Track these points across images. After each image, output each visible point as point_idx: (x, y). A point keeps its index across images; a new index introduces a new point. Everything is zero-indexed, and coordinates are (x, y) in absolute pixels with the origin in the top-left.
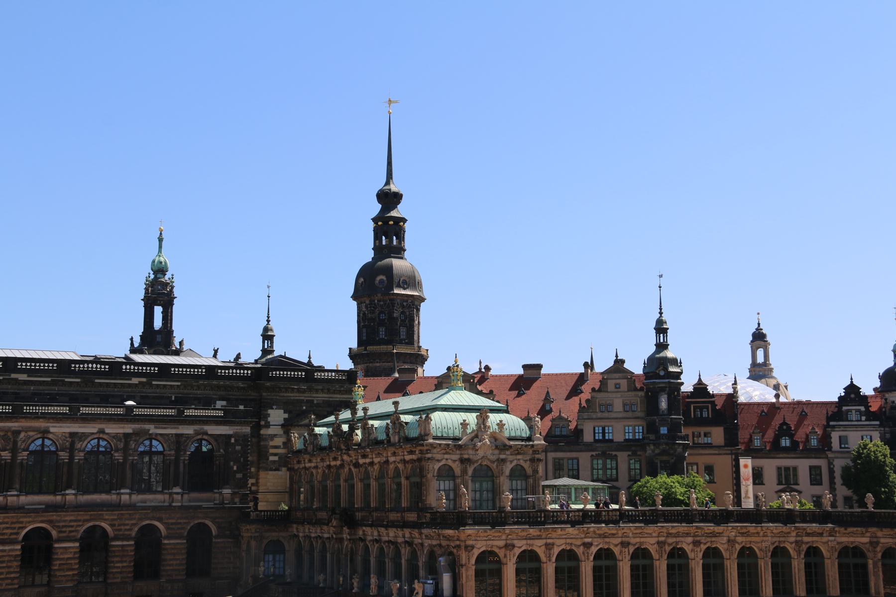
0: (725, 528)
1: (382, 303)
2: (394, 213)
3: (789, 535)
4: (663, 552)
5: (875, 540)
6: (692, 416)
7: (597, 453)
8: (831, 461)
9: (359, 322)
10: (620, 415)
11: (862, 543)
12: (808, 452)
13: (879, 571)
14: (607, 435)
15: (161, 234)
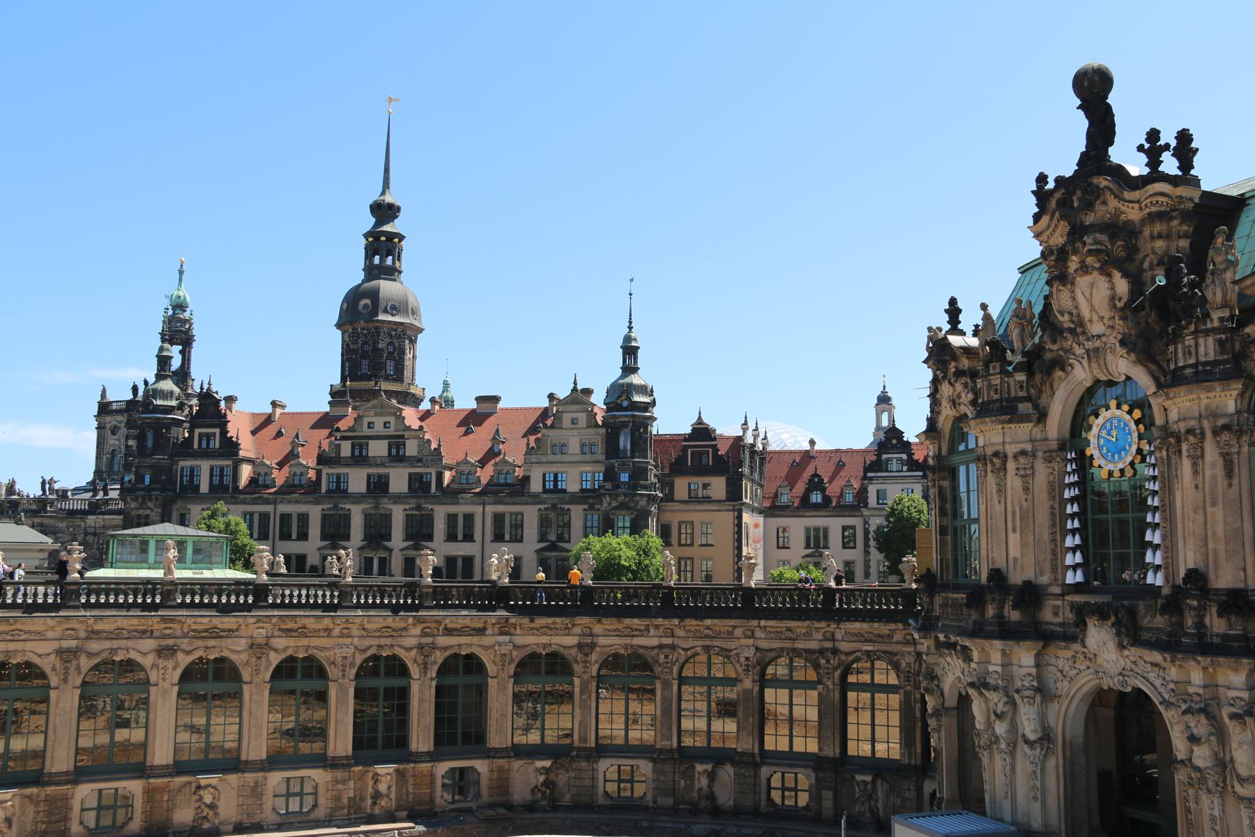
0: (241, 620)
1: (365, 332)
2: (387, 228)
3: (404, 634)
4: (72, 670)
5: (588, 640)
6: (689, 464)
7: (546, 506)
8: (867, 520)
9: (342, 355)
10: (577, 458)
11: (564, 647)
12: (843, 509)
13: (590, 697)
14: (559, 483)
15: (182, 266)
